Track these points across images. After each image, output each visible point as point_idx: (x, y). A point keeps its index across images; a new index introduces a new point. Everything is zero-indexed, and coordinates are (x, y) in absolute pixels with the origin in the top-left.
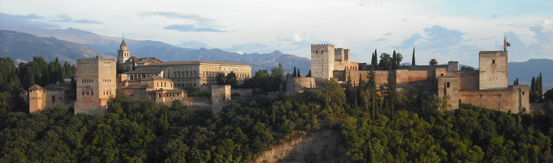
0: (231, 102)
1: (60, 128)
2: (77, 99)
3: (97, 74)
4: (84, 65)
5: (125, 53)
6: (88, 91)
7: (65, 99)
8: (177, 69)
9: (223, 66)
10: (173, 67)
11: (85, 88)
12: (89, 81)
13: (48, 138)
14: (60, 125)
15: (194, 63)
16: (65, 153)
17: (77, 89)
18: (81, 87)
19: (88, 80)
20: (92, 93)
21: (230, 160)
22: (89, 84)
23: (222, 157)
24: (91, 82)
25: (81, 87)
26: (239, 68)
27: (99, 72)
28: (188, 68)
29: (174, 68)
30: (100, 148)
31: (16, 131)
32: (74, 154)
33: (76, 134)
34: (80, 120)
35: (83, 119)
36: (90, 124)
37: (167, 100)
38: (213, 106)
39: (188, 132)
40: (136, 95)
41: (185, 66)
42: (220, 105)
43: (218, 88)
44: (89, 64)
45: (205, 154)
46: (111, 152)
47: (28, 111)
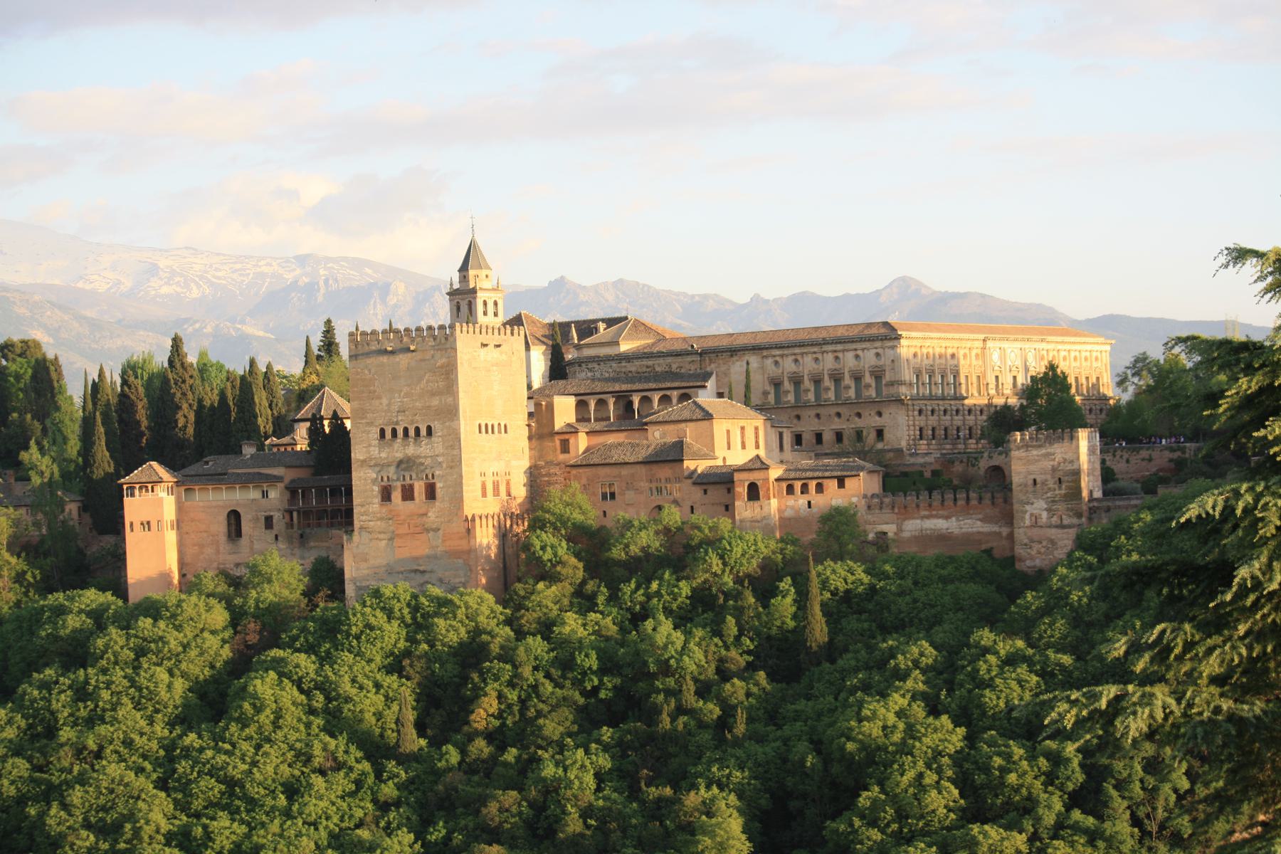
0: (1108, 510)
1: (305, 663)
2: (357, 524)
3: (450, 400)
4: (384, 359)
5: (485, 303)
6: (408, 481)
7: (290, 525)
8: (849, 360)
9: (998, 344)
10: (766, 357)
11: (392, 469)
12: (412, 433)
13: (258, 710)
14: (298, 645)
15: (866, 332)
16: (347, 775)
17: (354, 474)
18: (376, 465)
19: (406, 430)
20: (431, 493)
21: (1179, 786)
22: (411, 450)
23: (1141, 773)
24: (425, 441)
25: (376, 465)
26: (1059, 347)
27: (460, 389)
28: (840, 355)
29: (769, 361)
30: (514, 751)
31: (97, 681)
32: (389, 778)
33: (385, 684)
34: (390, 618)
35: (406, 611)
36: (445, 637)
37: (789, 513)
38: (1021, 530)
39: (935, 660)
40: (630, 495)
41: (826, 348)
42: (1057, 527)
43: (1040, 446)
44: (410, 355)
45: (1057, 760)
46: (578, 765)
47: (120, 589)
